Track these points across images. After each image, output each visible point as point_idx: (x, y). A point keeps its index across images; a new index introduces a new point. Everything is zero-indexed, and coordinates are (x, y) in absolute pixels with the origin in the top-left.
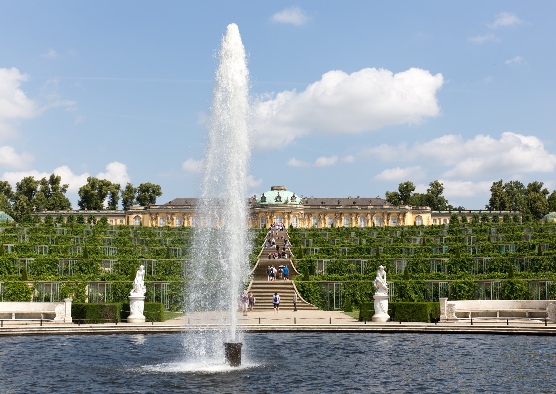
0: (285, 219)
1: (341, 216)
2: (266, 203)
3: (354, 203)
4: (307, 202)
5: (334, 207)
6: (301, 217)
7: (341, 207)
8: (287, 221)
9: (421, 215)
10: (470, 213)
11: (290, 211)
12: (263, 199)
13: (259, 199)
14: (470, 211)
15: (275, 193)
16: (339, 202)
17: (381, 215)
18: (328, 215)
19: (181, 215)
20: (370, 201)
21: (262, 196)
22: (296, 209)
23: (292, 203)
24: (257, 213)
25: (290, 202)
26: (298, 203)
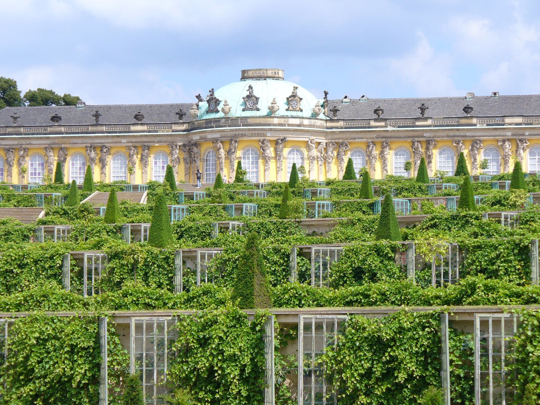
1: (427, 149)
3: (467, 109)
5: (408, 123)
6: (315, 153)
7: (429, 122)
8: (272, 164)
11: (282, 136)
12: (213, 102)
16: (423, 109)
18: (394, 146)
23: (289, 113)
26: (307, 113)
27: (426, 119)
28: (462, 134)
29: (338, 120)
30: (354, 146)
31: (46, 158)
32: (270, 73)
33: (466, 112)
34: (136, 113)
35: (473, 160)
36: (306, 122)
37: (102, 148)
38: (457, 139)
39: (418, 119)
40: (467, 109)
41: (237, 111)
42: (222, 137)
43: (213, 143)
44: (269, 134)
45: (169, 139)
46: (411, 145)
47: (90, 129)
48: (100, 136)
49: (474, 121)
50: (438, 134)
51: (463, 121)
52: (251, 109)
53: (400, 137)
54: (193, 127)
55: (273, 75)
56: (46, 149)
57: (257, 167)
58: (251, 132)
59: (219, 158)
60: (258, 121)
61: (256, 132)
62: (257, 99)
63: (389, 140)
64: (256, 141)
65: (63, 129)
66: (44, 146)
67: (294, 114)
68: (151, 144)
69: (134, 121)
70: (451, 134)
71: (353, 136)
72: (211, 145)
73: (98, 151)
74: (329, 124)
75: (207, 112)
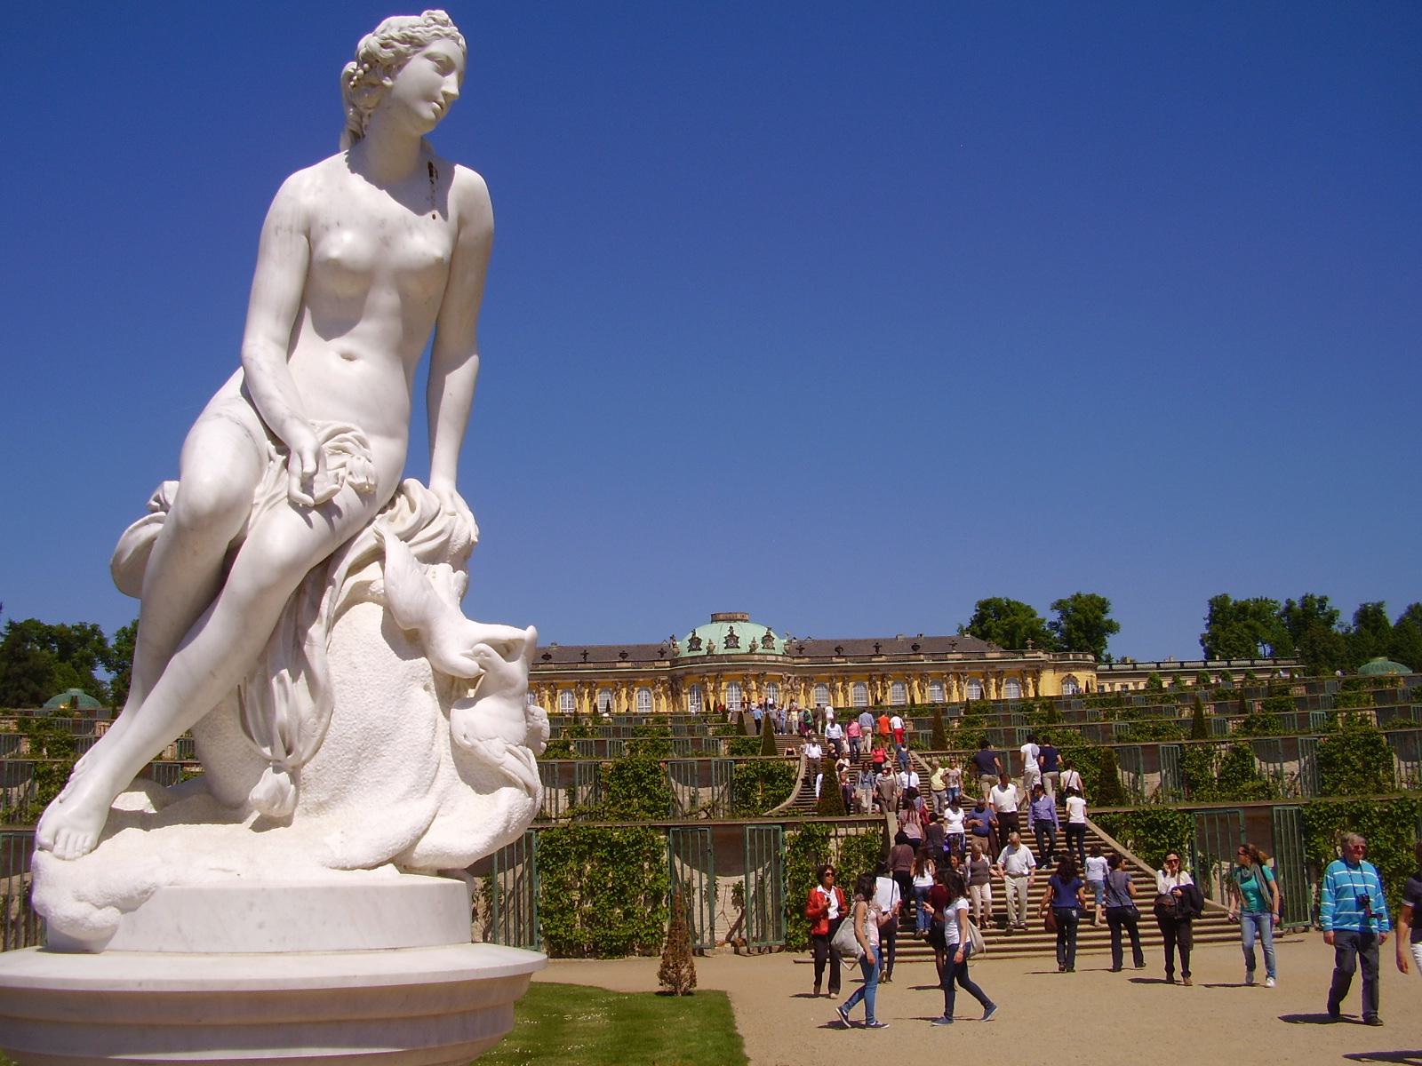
0: (749, 692)
2: (700, 653)
3: (915, 647)
4: (801, 649)
5: (867, 659)
7: (884, 658)
9: (1074, 674)
10: (1182, 667)
12: (695, 642)
13: (683, 646)
14: (1182, 663)
21: (690, 636)
25: (758, 651)
27: (881, 655)
29: (804, 657)
32: (739, 616)
33: (915, 650)
36: (780, 659)
37: (591, 684)
38: (907, 672)
40: (915, 647)
41: (720, 649)
49: (922, 657)
62: (738, 638)
70: (903, 667)
74: (796, 661)
75: (689, 651)
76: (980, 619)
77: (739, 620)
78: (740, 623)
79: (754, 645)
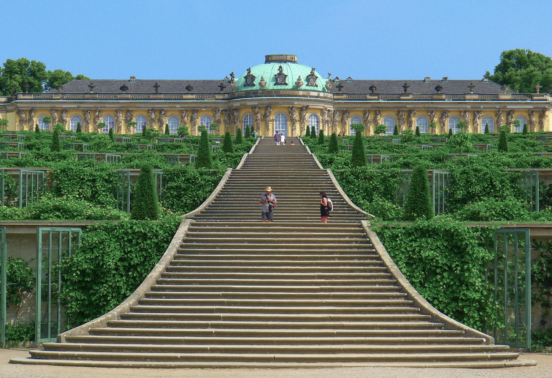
0: (293, 122)
1: (409, 116)
2: (254, 88)
3: (438, 88)
4: (340, 87)
6: (326, 118)
7: (411, 97)
8: (298, 125)
12: (249, 79)
15: (274, 68)
17: (493, 115)
18: (384, 114)
19: (81, 114)
20: (470, 85)
21: (246, 74)
22: (317, 99)
23: (308, 88)
24: (237, 109)
25: (304, 87)
26: (320, 88)
27: (408, 95)
28: (435, 106)
29: (343, 94)
30: (354, 113)
31: (116, 118)
33: (438, 90)
34: (187, 85)
35: (442, 125)
36: (322, 94)
39: (402, 95)
40: (438, 88)
41: (270, 86)
42: (259, 104)
43: (252, 108)
44: (296, 103)
45: (213, 105)
46: (397, 113)
47: (151, 96)
48: (158, 102)
49: (444, 97)
50: (417, 106)
51: (435, 97)
52: (281, 84)
53: (389, 108)
54: (232, 96)
55: (291, 59)
56: (116, 111)
57: (286, 128)
58: (284, 101)
59: (257, 120)
60: (288, 93)
61: (287, 101)
62: (286, 76)
63: (380, 109)
64: (286, 107)
65: (129, 96)
66: (115, 109)
67: (312, 88)
68: (199, 109)
69: (187, 91)
70: (427, 106)
71: (354, 106)
72: (250, 110)
73: (157, 114)
74: (335, 97)
75: (245, 86)
76: (503, 68)
77: (289, 61)
78: (290, 64)
79: (299, 83)
